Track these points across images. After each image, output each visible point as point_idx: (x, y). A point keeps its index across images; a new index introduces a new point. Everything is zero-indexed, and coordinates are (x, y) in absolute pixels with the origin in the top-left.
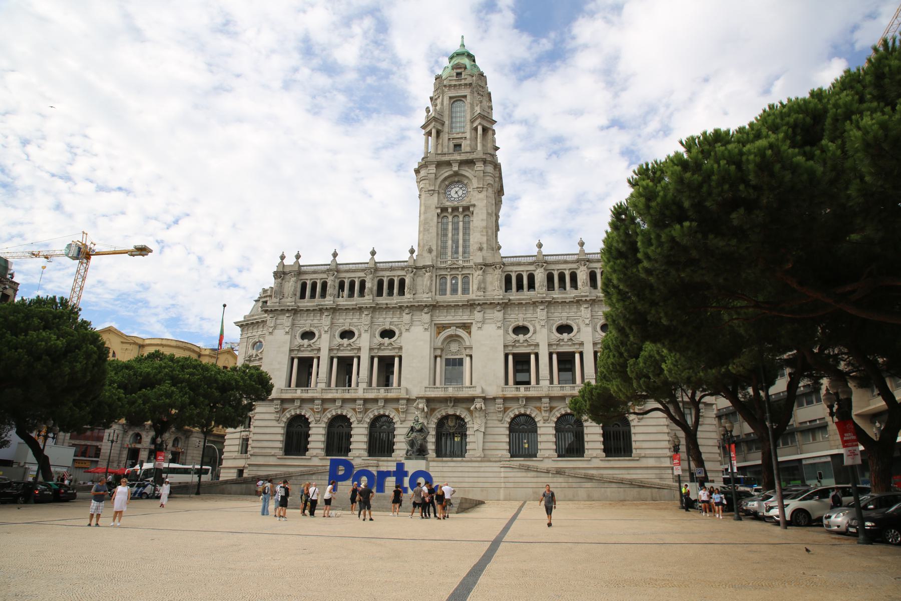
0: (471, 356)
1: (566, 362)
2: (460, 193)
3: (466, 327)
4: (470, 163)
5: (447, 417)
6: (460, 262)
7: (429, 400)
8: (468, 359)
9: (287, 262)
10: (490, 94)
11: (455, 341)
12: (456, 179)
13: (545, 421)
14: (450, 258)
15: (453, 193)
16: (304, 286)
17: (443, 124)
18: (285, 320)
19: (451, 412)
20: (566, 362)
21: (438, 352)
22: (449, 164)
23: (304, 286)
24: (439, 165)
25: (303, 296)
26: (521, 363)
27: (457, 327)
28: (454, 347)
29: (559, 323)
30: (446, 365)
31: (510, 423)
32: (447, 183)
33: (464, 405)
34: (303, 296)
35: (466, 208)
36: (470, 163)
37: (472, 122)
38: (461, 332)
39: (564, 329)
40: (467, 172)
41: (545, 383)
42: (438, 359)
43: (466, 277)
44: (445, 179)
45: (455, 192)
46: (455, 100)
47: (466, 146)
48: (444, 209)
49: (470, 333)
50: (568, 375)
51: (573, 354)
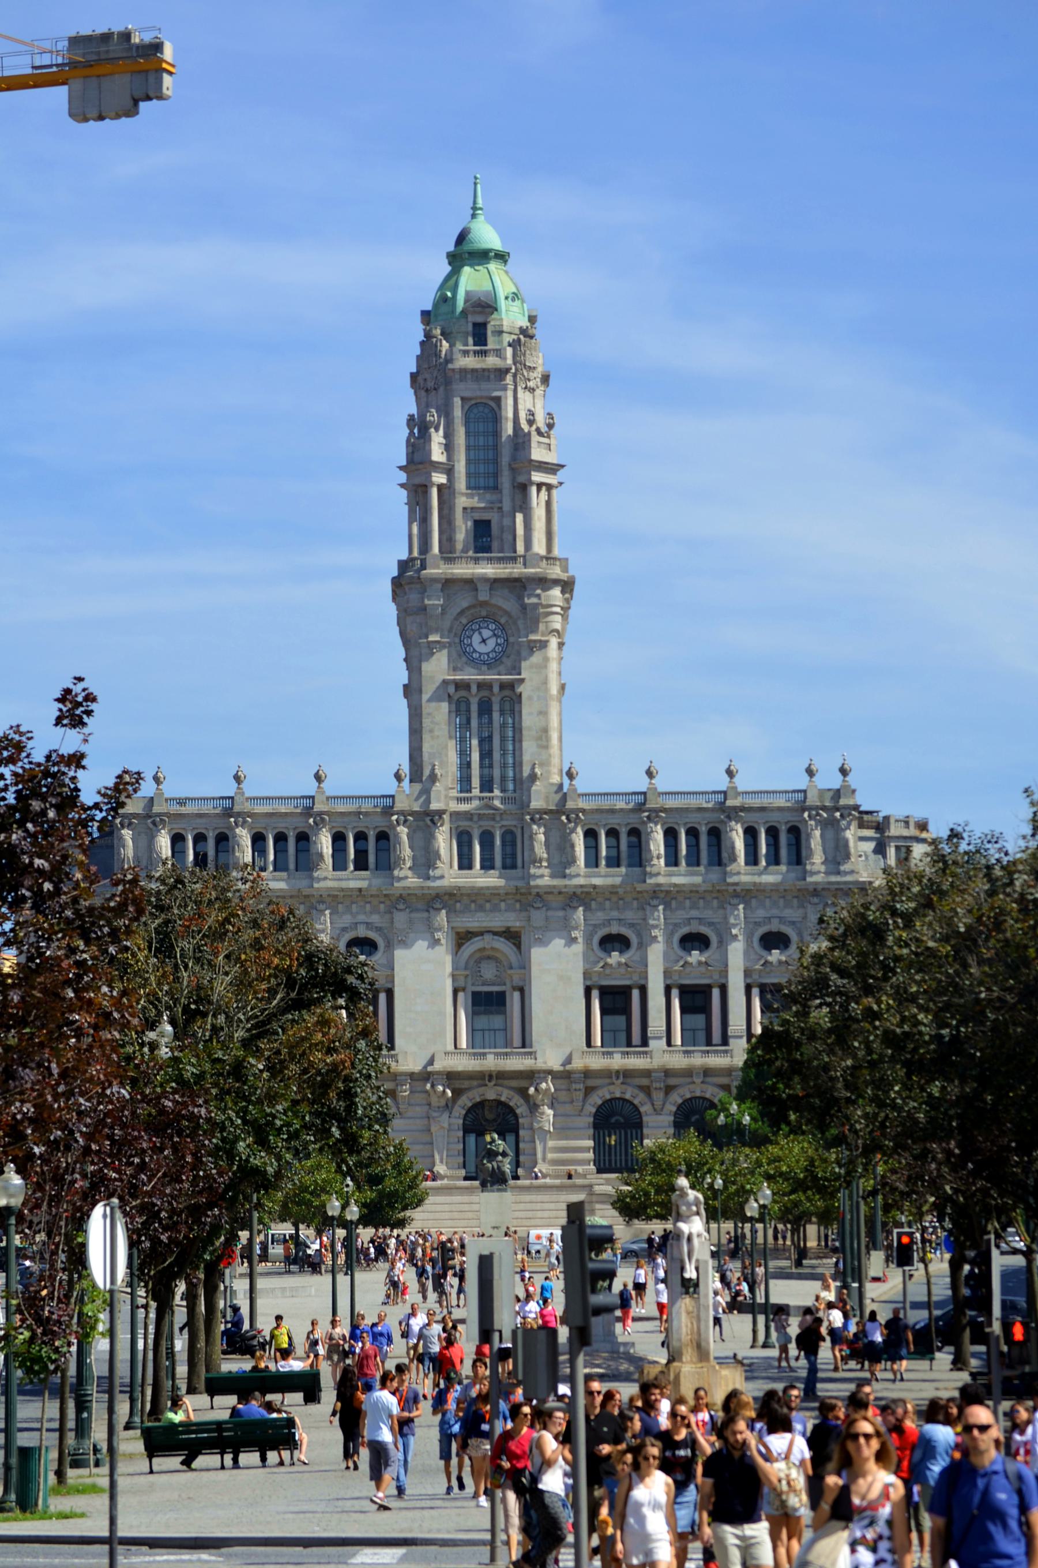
0: (522, 990)
1: (697, 999)
2: (491, 643)
3: (513, 936)
5: (480, 1105)
6: (497, 803)
7: (450, 1077)
8: (517, 995)
11: (489, 958)
12: (484, 613)
13: (657, 1112)
14: (476, 792)
15: (476, 639)
19: (491, 1094)
20: (697, 999)
21: (461, 983)
22: (470, 583)
26: (616, 1003)
27: (495, 933)
28: (489, 971)
29: (685, 930)
30: (474, 1004)
31: (596, 1116)
32: (464, 621)
33: (514, 1083)
38: (503, 946)
39: (694, 941)
41: (657, 1045)
42: (461, 995)
44: (462, 613)
49: (518, 946)
50: (699, 1019)
51: (709, 987)
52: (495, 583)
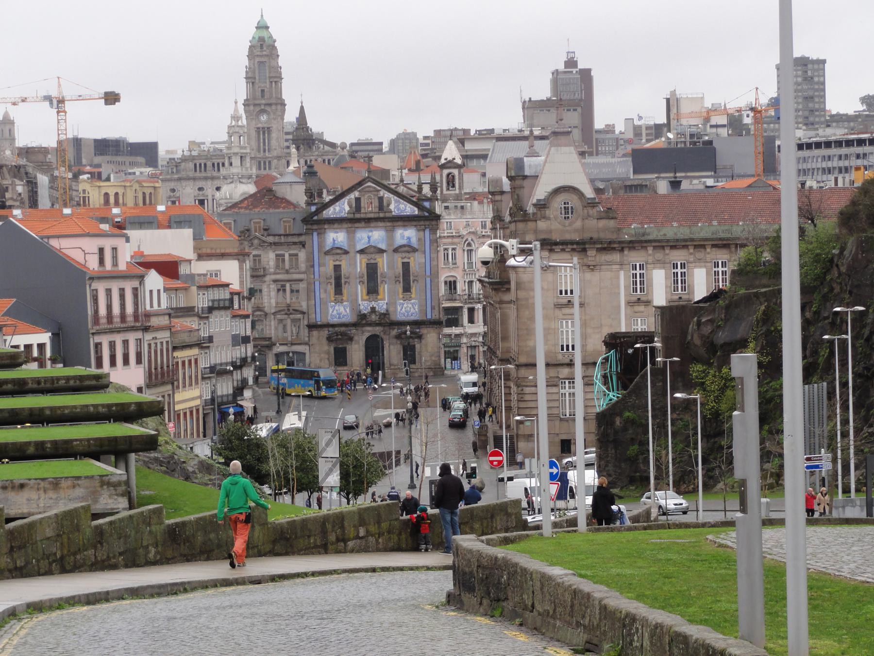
4: (270, 105)
9: (185, 153)
10: (278, 56)
16: (195, 165)
17: (255, 78)
18: (191, 183)
22: (259, 105)
23: (195, 165)
24: (255, 105)
25: (196, 171)
34: (196, 171)
35: (268, 128)
36: (270, 105)
37: (270, 78)
40: (268, 108)
43: (270, 162)
45: (264, 118)
46: (260, 63)
47: (267, 95)
48: (258, 128)
52: (265, 105)
